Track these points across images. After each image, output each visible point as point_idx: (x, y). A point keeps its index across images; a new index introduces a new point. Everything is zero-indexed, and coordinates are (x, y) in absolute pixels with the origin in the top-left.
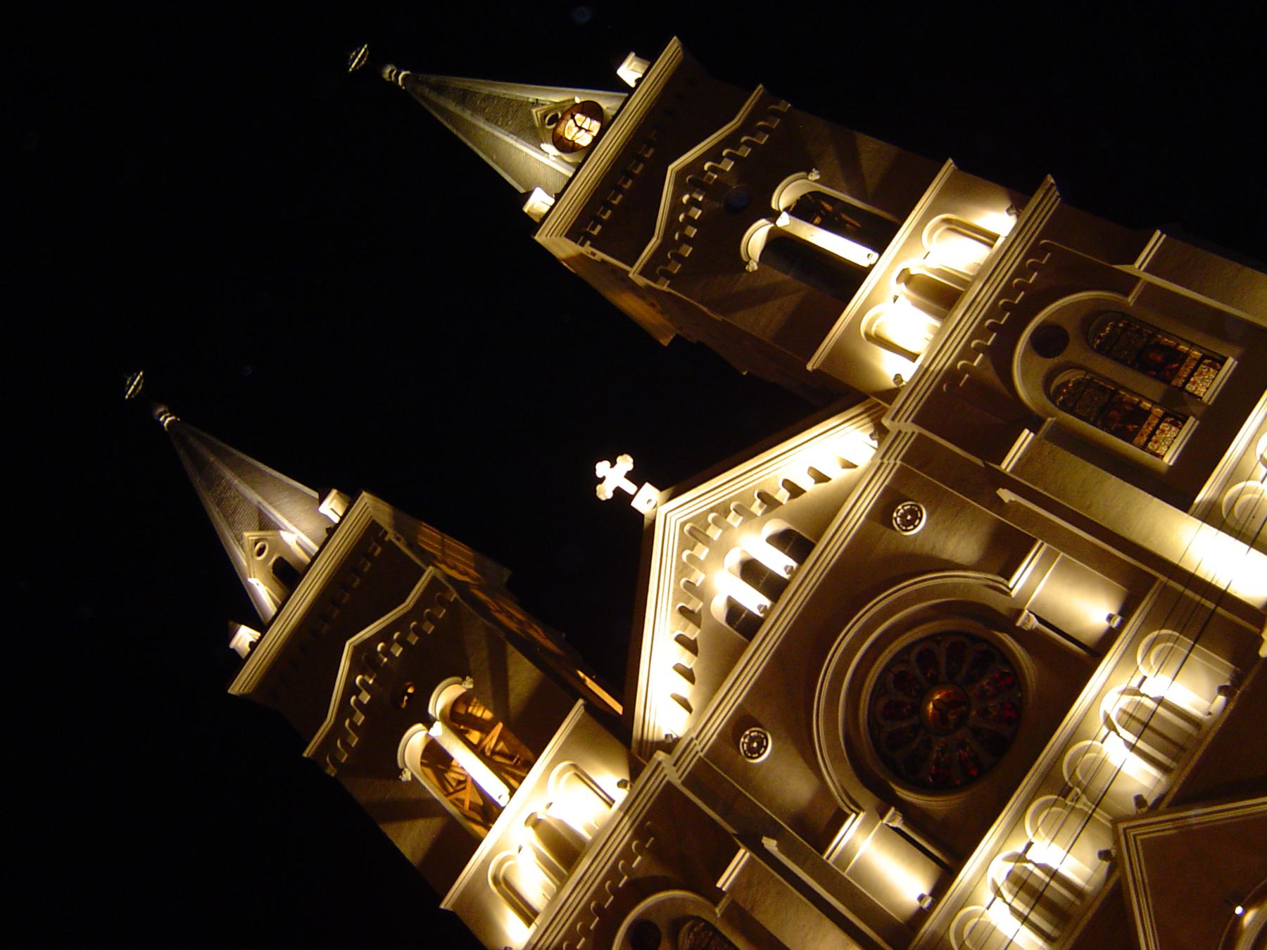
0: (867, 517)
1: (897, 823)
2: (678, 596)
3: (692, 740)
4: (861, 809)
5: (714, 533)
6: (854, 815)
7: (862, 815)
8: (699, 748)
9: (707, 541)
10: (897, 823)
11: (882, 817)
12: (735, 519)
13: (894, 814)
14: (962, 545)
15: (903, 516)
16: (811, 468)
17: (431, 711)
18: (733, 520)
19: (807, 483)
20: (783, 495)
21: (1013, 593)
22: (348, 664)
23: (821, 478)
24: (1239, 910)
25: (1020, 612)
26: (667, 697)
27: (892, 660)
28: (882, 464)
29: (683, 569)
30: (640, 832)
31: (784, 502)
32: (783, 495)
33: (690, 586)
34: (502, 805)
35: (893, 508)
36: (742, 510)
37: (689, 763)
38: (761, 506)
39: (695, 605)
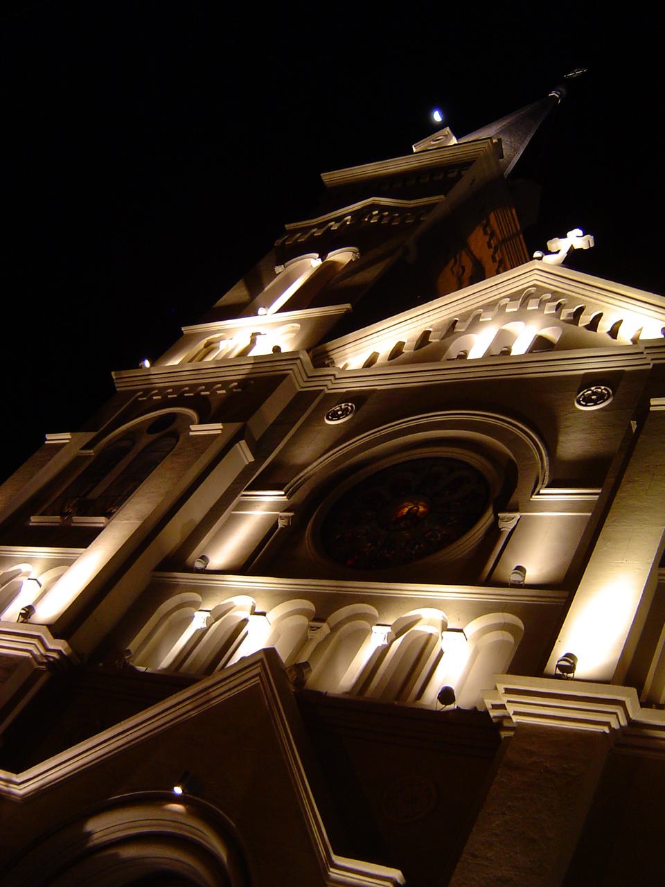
0: (585, 374)
1: (281, 524)
2: (464, 317)
3: (334, 375)
4: (289, 497)
5: (533, 306)
6: (283, 493)
7: (284, 499)
8: (331, 386)
9: (524, 304)
10: (281, 524)
11: (284, 511)
12: (550, 308)
13: (286, 517)
14: (573, 444)
15: (594, 393)
16: (622, 321)
17: (329, 254)
18: (549, 309)
19: (605, 326)
20: (585, 319)
21: (535, 498)
22: (359, 207)
23: (613, 333)
24: (178, 790)
25: (517, 510)
26: (369, 349)
27: (448, 459)
28: (642, 353)
29: (489, 306)
30: (243, 383)
31: (580, 325)
32: (585, 319)
33: (479, 316)
34: (259, 313)
35: (598, 384)
36: (559, 307)
37: (313, 386)
38: (569, 315)
39: (459, 328)
